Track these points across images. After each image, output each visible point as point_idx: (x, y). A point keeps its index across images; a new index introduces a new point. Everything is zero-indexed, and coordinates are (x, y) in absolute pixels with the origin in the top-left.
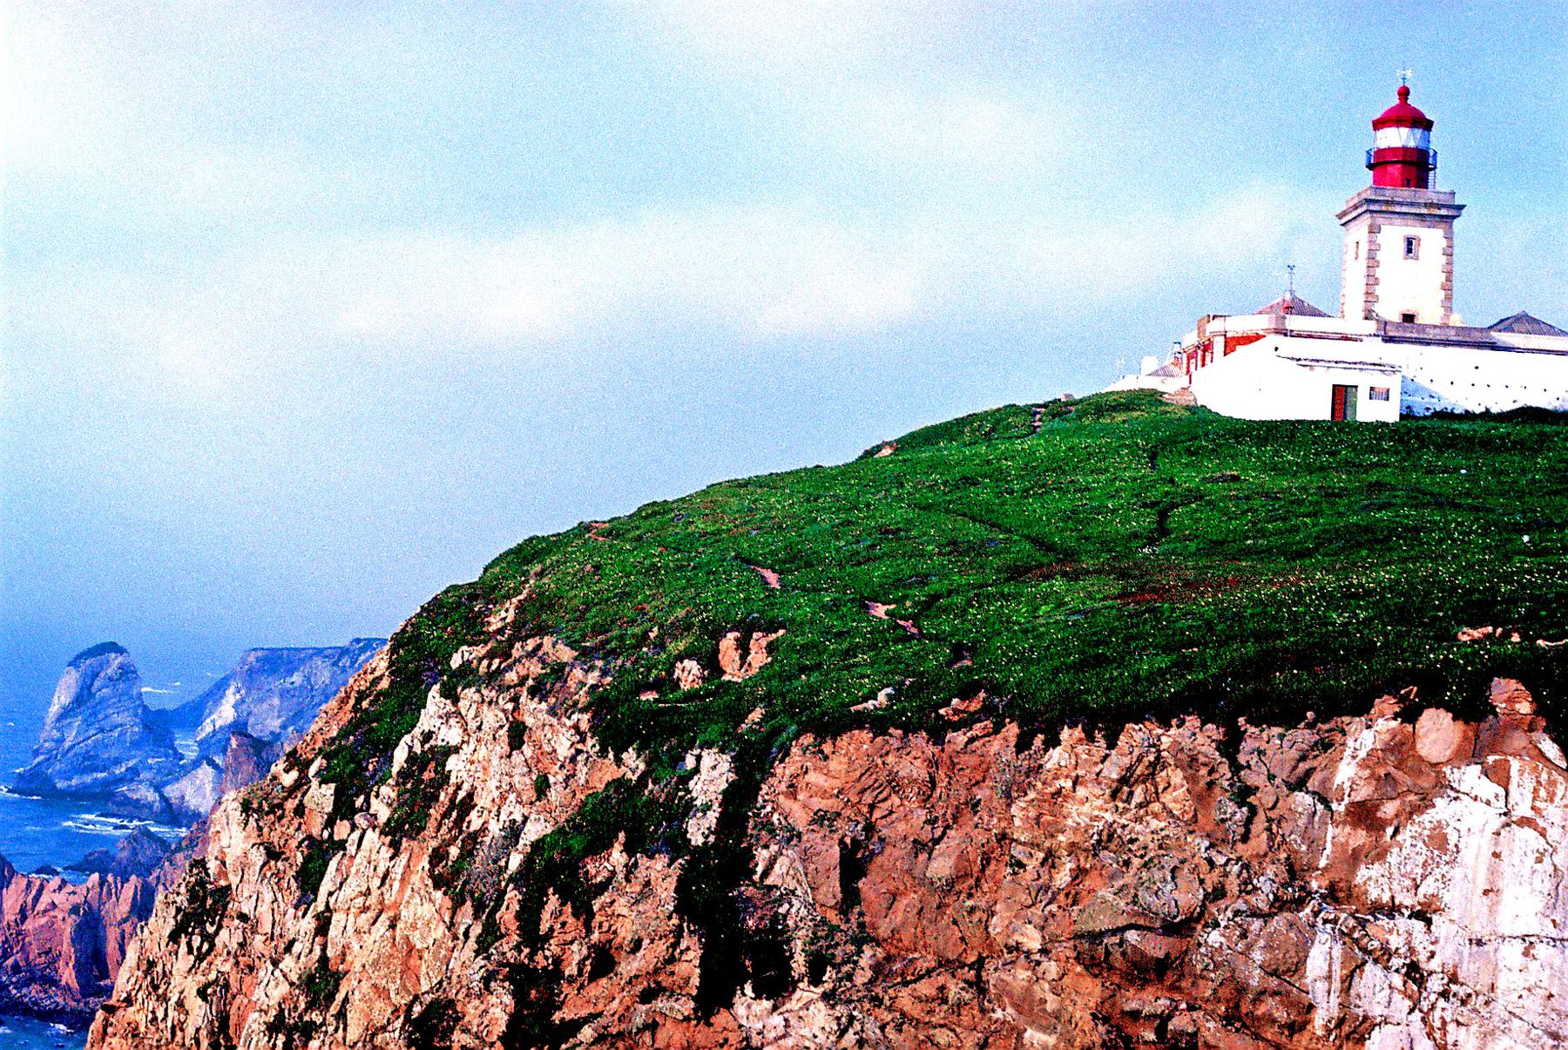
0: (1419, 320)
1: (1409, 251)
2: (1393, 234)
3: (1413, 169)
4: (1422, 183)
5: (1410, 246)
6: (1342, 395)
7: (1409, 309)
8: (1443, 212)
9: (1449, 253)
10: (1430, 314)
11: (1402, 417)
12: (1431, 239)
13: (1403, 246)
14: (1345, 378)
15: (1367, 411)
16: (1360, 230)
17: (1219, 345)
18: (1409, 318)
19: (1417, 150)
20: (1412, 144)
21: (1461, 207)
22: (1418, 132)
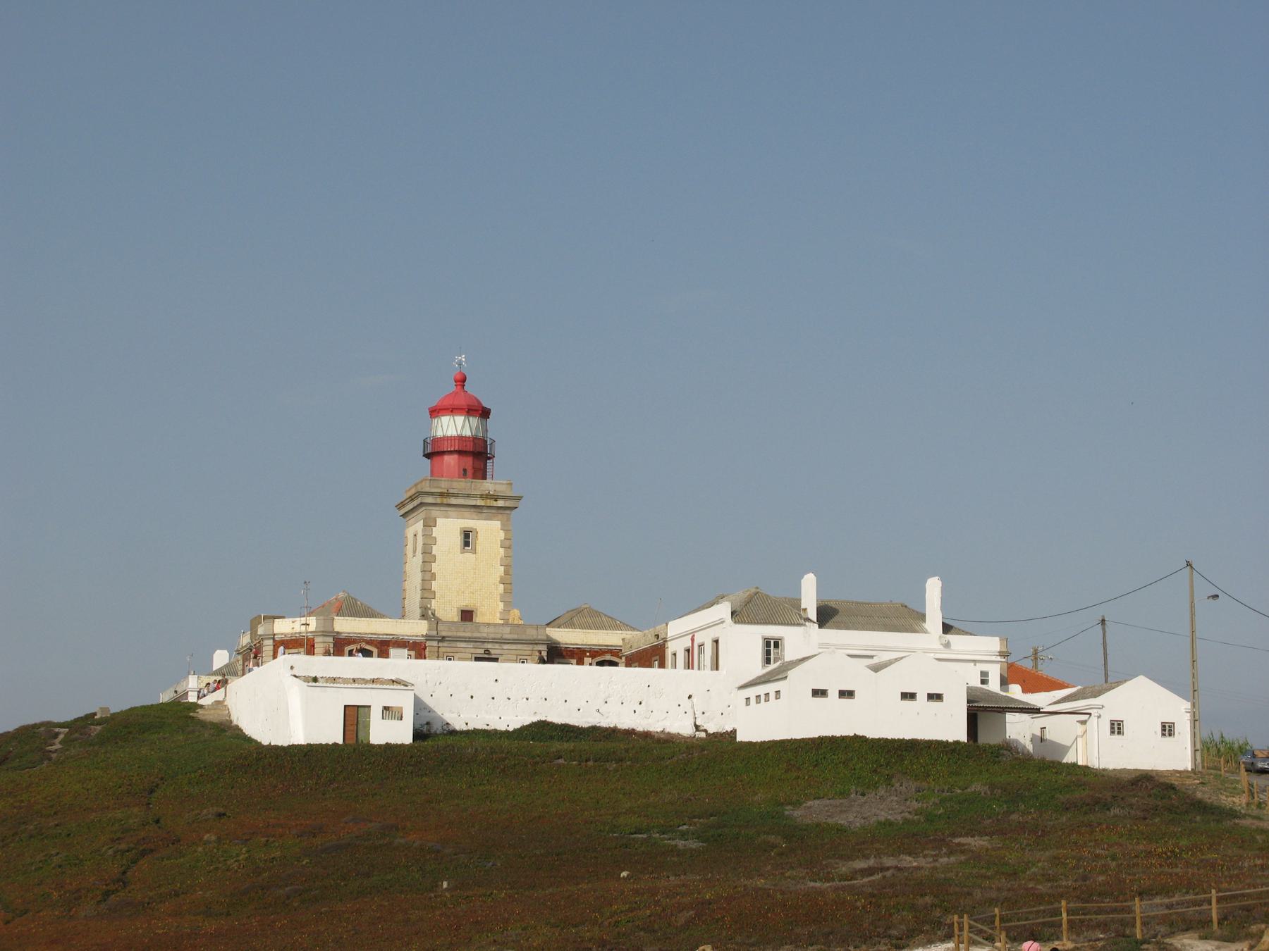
0: (478, 619)
1: (467, 544)
2: (448, 528)
3: (468, 462)
4: (481, 473)
6: (354, 717)
7: (466, 603)
8: (500, 503)
10: (491, 611)
11: (418, 735)
12: (490, 531)
13: (458, 540)
14: (356, 697)
15: (384, 732)
16: (415, 527)
17: (268, 646)
18: (467, 615)
19: (474, 439)
21: (518, 499)
22: (475, 421)
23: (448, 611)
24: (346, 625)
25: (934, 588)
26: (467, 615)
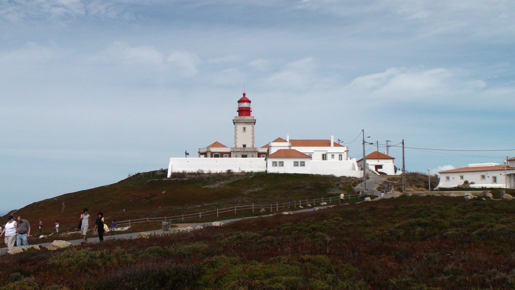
0: (247, 146)
2: (240, 127)
5: (244, 128)
7: (244, 144)
9: (253, 131)
12: (249, 127)
13: (242, 129)
18: (244, 146)
20: (244, 106)
21: (255, 120)
23: (240, 145)
24: (213, 150)
25: (332, 137)
26: (244, 146)
